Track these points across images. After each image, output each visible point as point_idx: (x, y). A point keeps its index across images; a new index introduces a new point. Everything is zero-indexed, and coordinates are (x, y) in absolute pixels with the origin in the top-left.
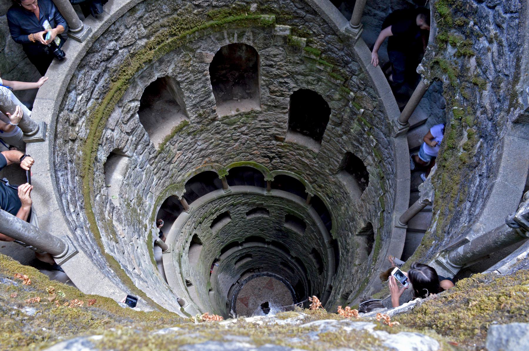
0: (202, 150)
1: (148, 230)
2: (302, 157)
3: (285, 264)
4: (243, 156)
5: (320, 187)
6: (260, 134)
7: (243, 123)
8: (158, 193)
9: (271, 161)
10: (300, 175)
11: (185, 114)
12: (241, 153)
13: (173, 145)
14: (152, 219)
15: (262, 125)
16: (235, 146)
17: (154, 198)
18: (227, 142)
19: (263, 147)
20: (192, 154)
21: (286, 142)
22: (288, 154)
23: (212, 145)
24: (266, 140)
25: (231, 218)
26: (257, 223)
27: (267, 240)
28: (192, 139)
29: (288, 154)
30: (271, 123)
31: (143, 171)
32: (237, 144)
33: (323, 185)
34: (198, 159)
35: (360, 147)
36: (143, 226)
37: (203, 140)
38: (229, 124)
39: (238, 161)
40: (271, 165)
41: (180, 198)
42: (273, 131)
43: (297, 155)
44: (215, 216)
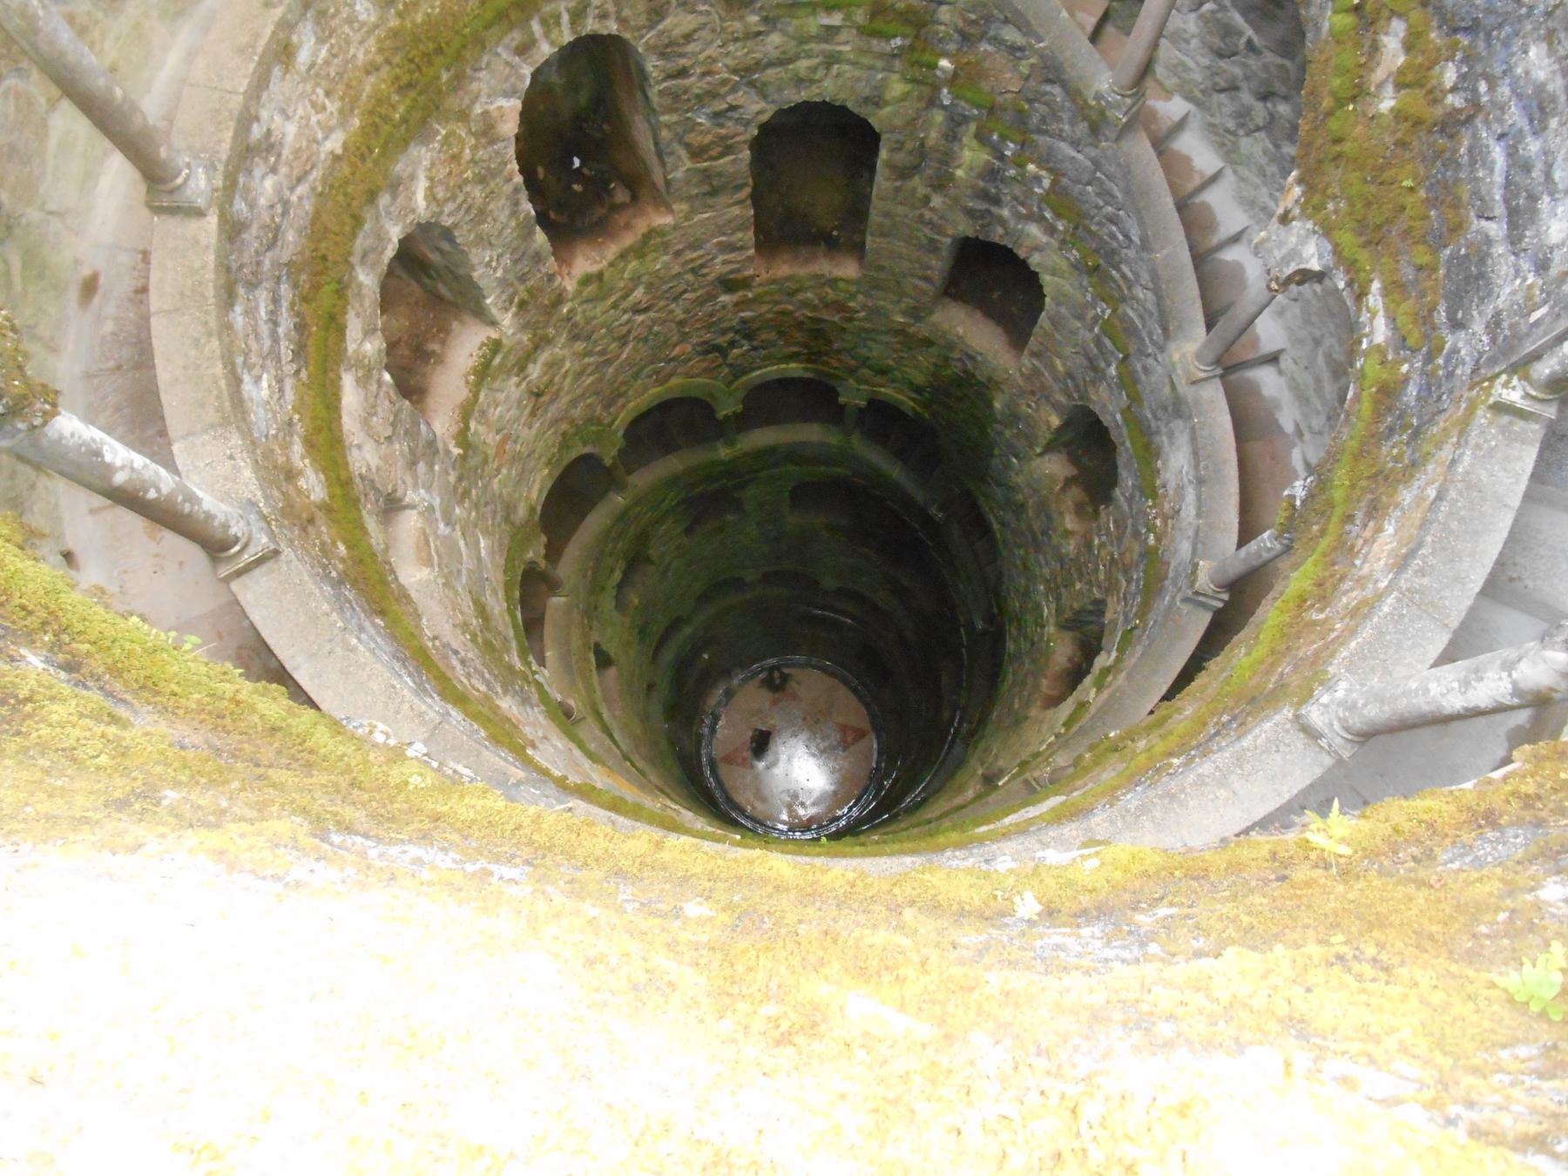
11: (481, 314)
25: (651, 562)
30: (708, 245)
35: (994, 210)
40: (726, 370)
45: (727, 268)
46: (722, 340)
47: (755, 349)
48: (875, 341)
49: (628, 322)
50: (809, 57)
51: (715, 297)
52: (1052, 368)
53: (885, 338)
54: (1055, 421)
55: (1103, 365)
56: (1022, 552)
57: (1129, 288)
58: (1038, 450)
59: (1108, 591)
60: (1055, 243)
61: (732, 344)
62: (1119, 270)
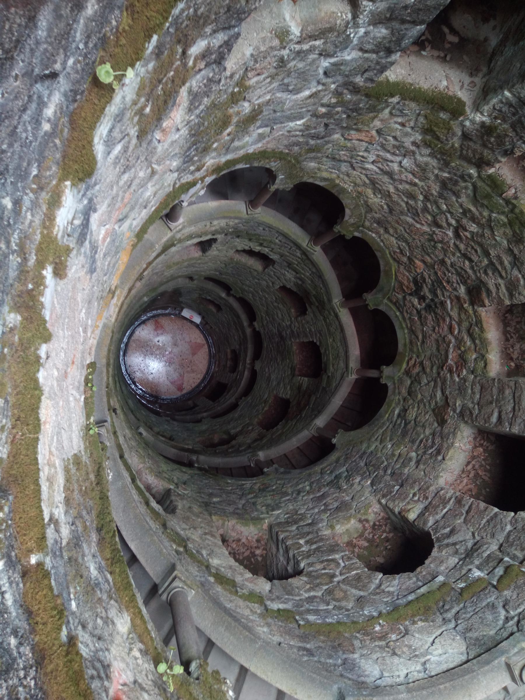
0: (390, 174)
1: (198, 175)
2: (458, 347)
3: (236, 358)
4: (399, 248)
6: (471, 260)
7: (490, 220)
8: (271, 146)
9: (411, 294)
11: (485, 93)
12: (406, 242)
13: (391, 113)
14: (217, 169)
15: (499, 258)
16: (418, 226)
17: (260, 145)
18: (425, 209)
19: (439, 273)
20: (373, 162)
21: (475, 312)
22: (448, 320)
23: (407, 186)
24: (458, 274)
25: (264, 269)
26: (276, 304)
27: (255, 324)
28: (414, 143)
29: (448, 320)
30: (515, 272)
31: (319, 83)
32: (426, 228)
33: (419, 396)
34: (363, 177)
36: (200, 160)
37: (418, 166)
38: (475, 200)
39: (385, 242)
40: (400, 297)
41: (273, 188)
43: (456, 338)
44: (257, 249)
46: (426, 291)
47: (419, 312)
48: (435, 386)
49: (449, 225)
51: (465, 283)
52: (453, 514)
53: (439, 394)
54: (412, 516)
55: (477, 562)
56: (308, 488)
58: (383, 501)
59: (309, 574)
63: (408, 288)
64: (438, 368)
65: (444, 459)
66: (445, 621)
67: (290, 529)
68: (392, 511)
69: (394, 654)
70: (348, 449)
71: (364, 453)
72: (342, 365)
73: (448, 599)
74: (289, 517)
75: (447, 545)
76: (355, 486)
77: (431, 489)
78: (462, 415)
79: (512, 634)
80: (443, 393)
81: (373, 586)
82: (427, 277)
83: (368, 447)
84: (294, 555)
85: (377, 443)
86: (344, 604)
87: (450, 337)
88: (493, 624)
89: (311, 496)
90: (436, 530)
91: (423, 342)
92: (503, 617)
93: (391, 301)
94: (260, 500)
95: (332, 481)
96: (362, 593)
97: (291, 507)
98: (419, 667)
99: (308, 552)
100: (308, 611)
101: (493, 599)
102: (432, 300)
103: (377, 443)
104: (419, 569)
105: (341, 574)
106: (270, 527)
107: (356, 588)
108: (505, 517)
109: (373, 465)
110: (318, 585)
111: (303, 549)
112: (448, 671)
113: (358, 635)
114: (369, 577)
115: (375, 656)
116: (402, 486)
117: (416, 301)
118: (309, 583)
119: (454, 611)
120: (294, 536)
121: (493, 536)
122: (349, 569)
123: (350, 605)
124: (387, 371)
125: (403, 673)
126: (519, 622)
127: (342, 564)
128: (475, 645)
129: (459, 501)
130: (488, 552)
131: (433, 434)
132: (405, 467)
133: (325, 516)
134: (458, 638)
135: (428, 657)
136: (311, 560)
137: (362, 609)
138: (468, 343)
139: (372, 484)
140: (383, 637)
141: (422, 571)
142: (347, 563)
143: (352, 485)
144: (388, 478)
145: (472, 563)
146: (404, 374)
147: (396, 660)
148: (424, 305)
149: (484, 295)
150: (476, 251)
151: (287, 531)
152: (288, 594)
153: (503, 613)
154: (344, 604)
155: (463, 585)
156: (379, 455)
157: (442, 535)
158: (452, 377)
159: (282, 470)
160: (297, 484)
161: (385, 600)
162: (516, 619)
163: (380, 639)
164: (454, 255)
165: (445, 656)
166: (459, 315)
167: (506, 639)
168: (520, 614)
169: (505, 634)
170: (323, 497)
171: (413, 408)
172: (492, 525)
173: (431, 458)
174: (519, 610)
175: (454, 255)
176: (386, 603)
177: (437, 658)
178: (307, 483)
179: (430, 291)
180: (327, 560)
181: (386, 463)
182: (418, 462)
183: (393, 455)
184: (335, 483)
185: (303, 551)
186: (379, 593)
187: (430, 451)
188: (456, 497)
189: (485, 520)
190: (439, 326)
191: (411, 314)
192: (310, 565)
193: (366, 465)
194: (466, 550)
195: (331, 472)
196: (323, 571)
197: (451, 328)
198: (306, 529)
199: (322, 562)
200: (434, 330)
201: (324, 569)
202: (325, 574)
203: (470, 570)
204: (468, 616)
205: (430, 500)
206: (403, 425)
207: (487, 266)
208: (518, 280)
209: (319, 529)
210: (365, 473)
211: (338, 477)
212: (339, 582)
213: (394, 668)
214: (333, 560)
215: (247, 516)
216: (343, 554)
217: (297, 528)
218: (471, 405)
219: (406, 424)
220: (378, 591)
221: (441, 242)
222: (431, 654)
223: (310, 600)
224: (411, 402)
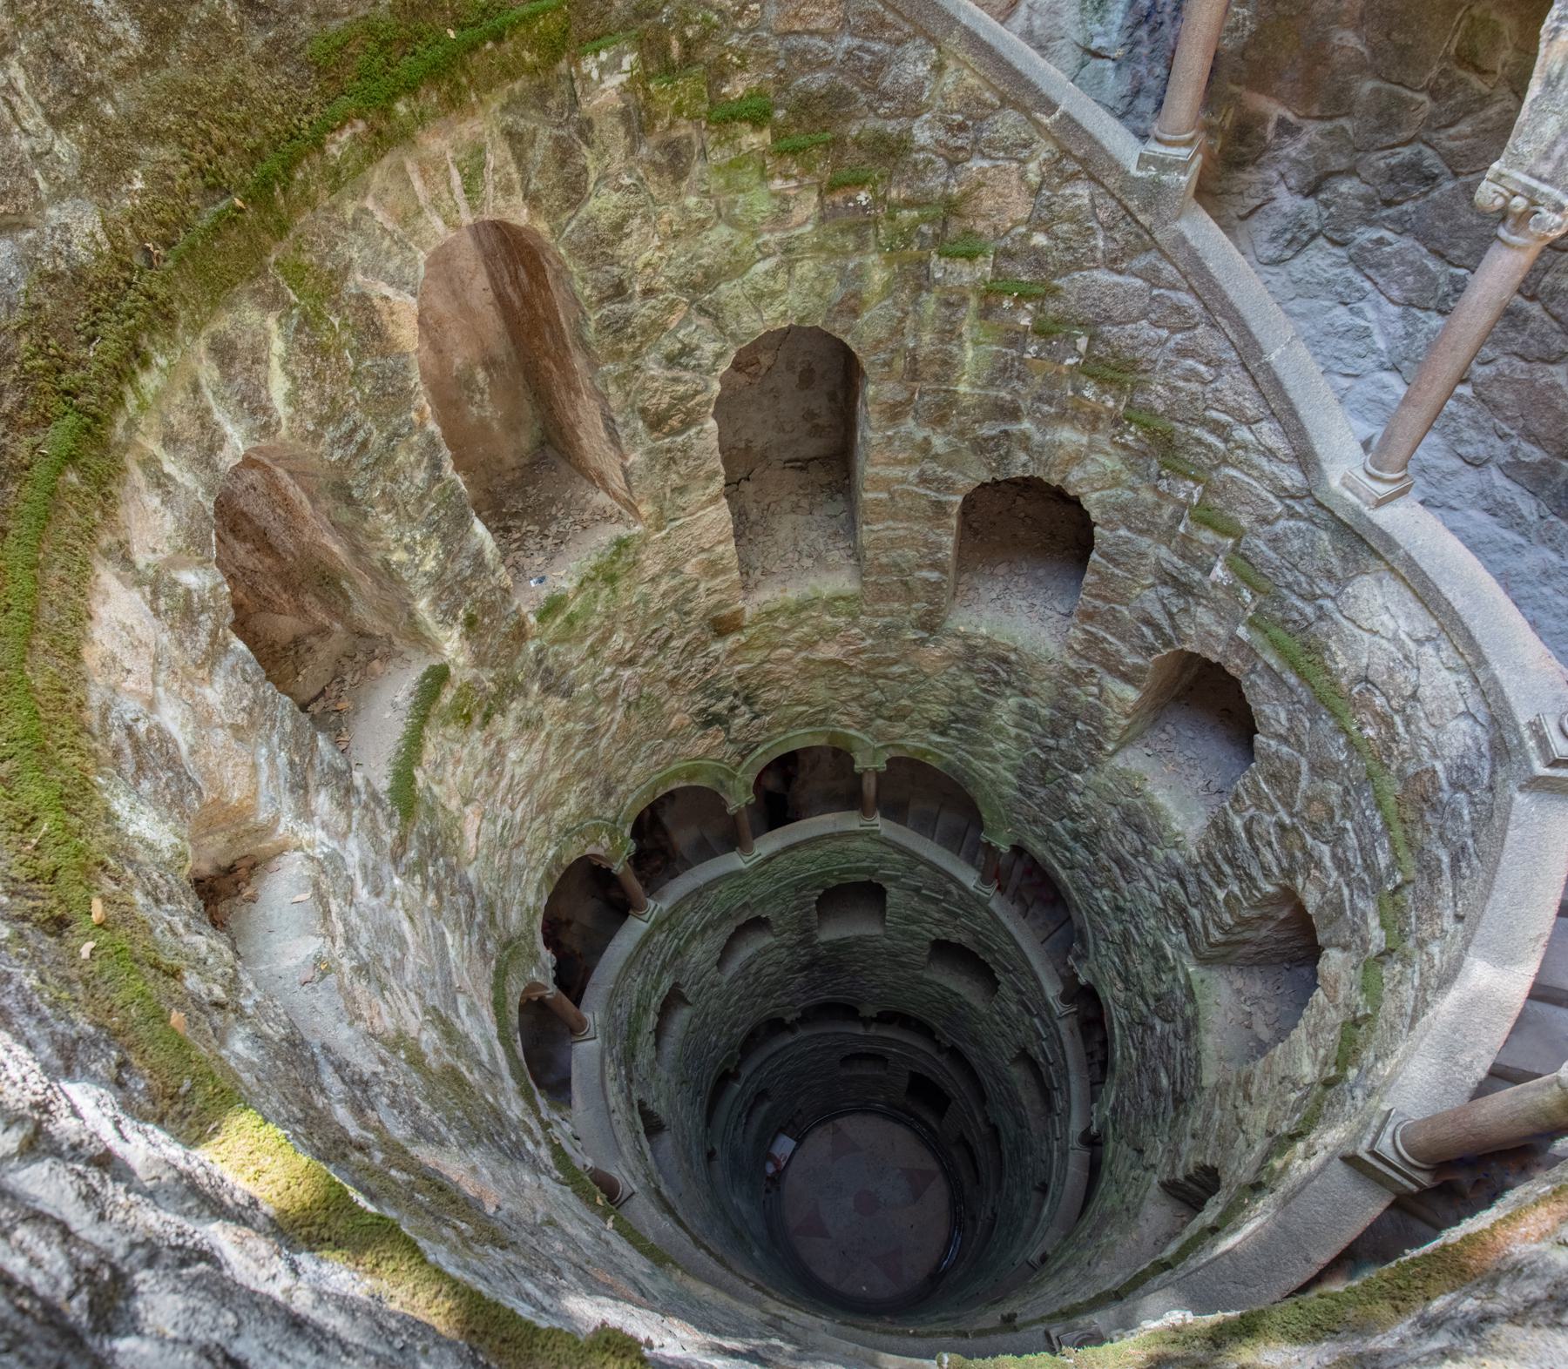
5: (901, 715)
6: (670, 637)
9: (728, 731)
10: (823, 722)
15: (664, 595)
22: (767, 666)
24: (692, 655)
33: (904, 702)
40: (731, 748)
42: (703, 602)
43: (799, 650)
45: (716, 598)
46: (720, 707)
47: (757, 716)
48: (885, 677)
50: (766, 256)
51: (705, 644)
52: (1112, 621)
55: (1198, 576)
57: (1226, 441)
58: (1110, 747)
59: (1289, 873)
60: (1102, 439)
61: (732, 709)
62: (1205, 423)
63: (715, 737)
64: (852, 674)
65: (1015, 650)
66: (1322, 615)
67: (1198, 920)
68: (1126, 730)
69: (1414, 696)
70: (1018, 821)
71: (1021, 789)
72: (858, 844)
73: (1279, 615)
74: (1175, 925)
75: (1175, 627)
76: (1089, 801)
77: (1073, 666)
78: (932, 629)
79: (1320, 505)
80: (896, 662)
81: (1285, 749)
82: (697, 707)
83: (1009, 784)
84: (1252, 907)
85: (999, 767)
86: (1334, 800)
87: (797, 659)
88: (1309, 536)
89: (1122, 883)
90: (1150, 650)
91: (807, 703)
92: (1292, 523)
93: (739, 764)
94: (1149, 987)
95: (1086, 846)
96: (1304, 768)
97: (1152, 921)
98: (1428, 649)
99: (1241, 881)
100: (1369, 867)
101: (1260, 543)
102: (736, 694)
103: (999, 767)
104: (1232, 672)
105: (1274, 811)
106: (1204, 961)
107: (1297, 781)
108: (1105, 540)
109: (1043, 772)
110: (1308, 854)
111: (1236, 890)
112: (1420, 599)
113: (1394, 767)
114: (1267, 758)
115: (1430, 733)
116: (1075, 718)
117: (739, 722)
118: (1308, 871)
119: (1299, 603)
120: (1212, 910)
121: (1142, 555)
122: (1259, 797)
123: (1335, 787)
124: (861, 762)
125: (1451, 678)
126: (1292, 497)
127: (1252, 811)
128: (1356, 561)
129: (1089, 616)
130: (1175, 559)
131: (970, 669)
132: (1038, 714)
133: (1159, 854)
134: (1349, 589)
135: (1403, 636)
136: (1255, 872)
137: (1338, 764)
138: (806, 629)
139: (1078, 770)
140: (1384, 720)
141: (1234, 665)
142: (1248, 802)
143: (1086, 806)
144: (1063, 743)
145: (1200, 583)
146: (866, 733)
147: (1426, 692)
148: (743, 708)
149: (725, 612)
150: (655, 631)
151: (1205, 927)
152: (1342, 912)
153: (1281, 525)
154: (1334, 800)
155: (1246, 595)
156: (1020, 762)
157: (1157, 638)
158: (864, 651)
159: (1076, 947)
160: (1102, 913)
161: (1308, 725)
162: (1288, 502)
163: (1390, 725)
164: (660, 666)
165: (1393, 609)
166: (759, 648)
167: (1332, 512)
168: (1278, 497)
169: (1323, 515)
170: (1120, 861)
171: (927, 711)
172: (1122, 559)
173: (1016, 673)
174: (1272, 499)
175: (660, 666)
176: (1313, 721)
177: (1401, 622)
178: (1097, 894)
179: (720, 699)
180: (1251, 839)
181: (1036, 750)
182: (1025, 694)
183: (1018, 736)
184: (1090, 840)
185: (1241, 889)
186: (1298, 738)
187: (1004, 675)
188: (1082, 622)
189: (1117, 571)
190: (779, 680)
191: (761, 728)
192: (1267, 874)
193: (1044, 786)
194: (1178, 596)
195: (1067, 849)
196: (1276, 846)
197: (781, 660)
198: (1192, 887)
199: (1256, 850)
200: (787, 688)
201: (1270, 844)
202: (1280, 840)
203: (1214, 585)
204: (1303, 579)
205: (1093, 666)
206: (960, 726)
207: (678, 612)
208: (701, 563)
209: (1189, 862)
210: (1059, 786)
211: (1076, 835)
212: (1292, 815)
213: (1445, 693)
214: (1248, 830)
215: (1189, 1010)
216: (1230, 812)
217: (1195, 905)
218: (913, 615)
219: (957, 720)
220: (1292, 740)
221: (640, 690)
222: (1395, 633)
223: (1342, 865)
224: (916, 716)
